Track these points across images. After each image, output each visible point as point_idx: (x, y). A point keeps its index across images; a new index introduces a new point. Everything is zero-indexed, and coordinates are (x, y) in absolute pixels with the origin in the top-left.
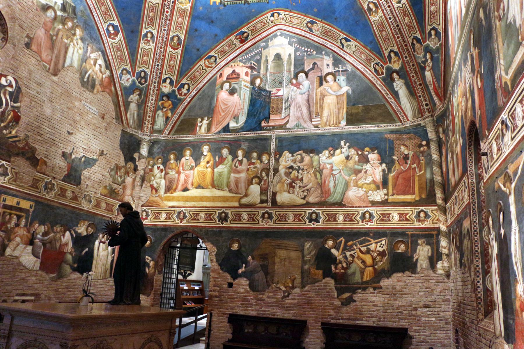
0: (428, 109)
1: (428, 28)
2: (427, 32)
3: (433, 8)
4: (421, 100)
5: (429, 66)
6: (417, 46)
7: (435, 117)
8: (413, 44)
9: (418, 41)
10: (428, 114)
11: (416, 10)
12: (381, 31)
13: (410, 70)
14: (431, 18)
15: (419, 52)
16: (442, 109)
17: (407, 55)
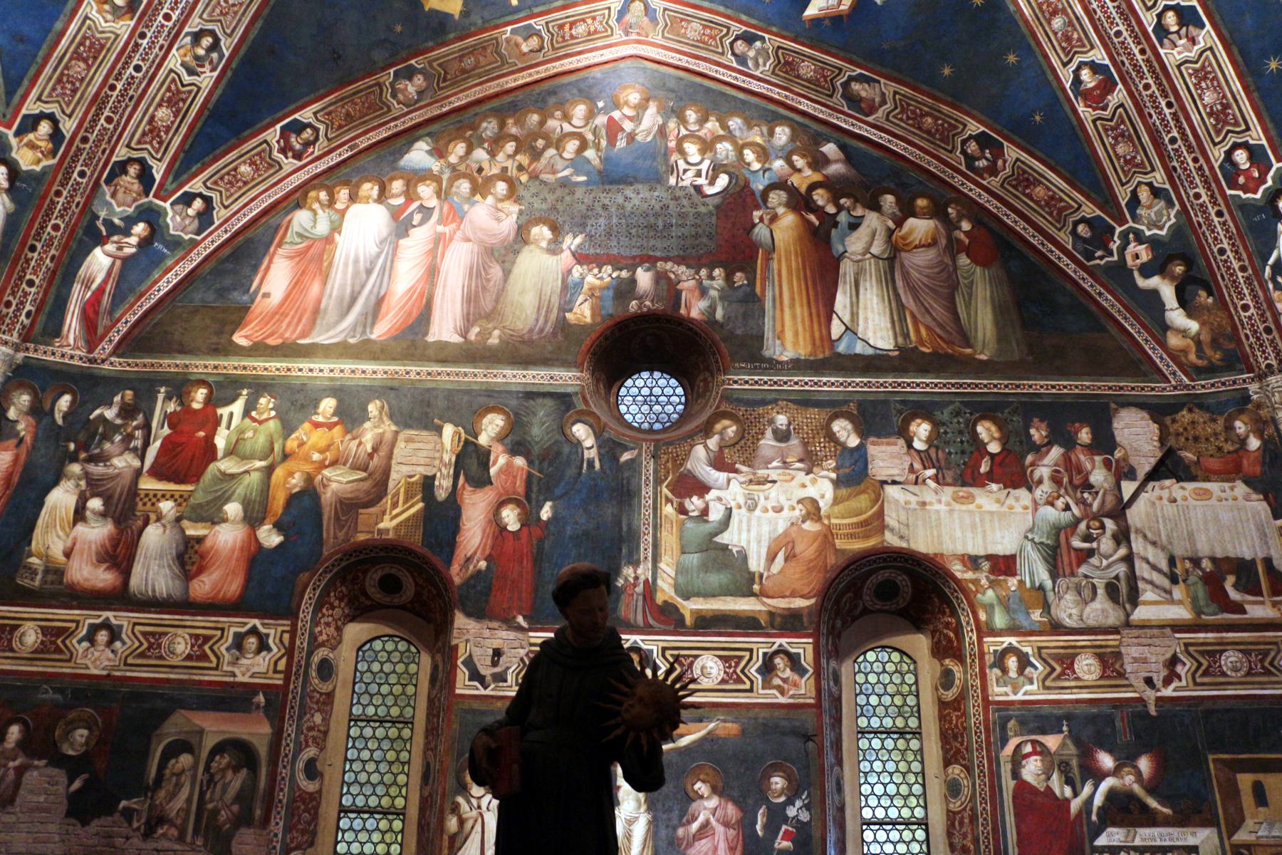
0: (24, 327)
1: (196, 185)
2: (186, 188)
3: (245, 169)
4: (26, 294)
5: (120, 249)
6: (130, 179)
7: (20, 355)
8: (122, 167)
9: (145, 177)
10: (15, 338)
11: (209, 130)
12: (77, 56)
13: (65, 209)
14: (222, 178)
15: (120, 195)
16: (76, 362)
17: (88, 173)
